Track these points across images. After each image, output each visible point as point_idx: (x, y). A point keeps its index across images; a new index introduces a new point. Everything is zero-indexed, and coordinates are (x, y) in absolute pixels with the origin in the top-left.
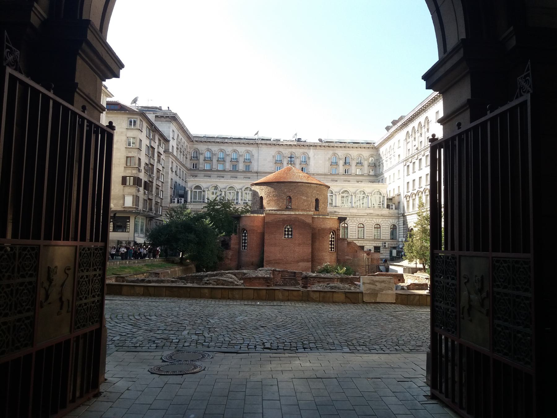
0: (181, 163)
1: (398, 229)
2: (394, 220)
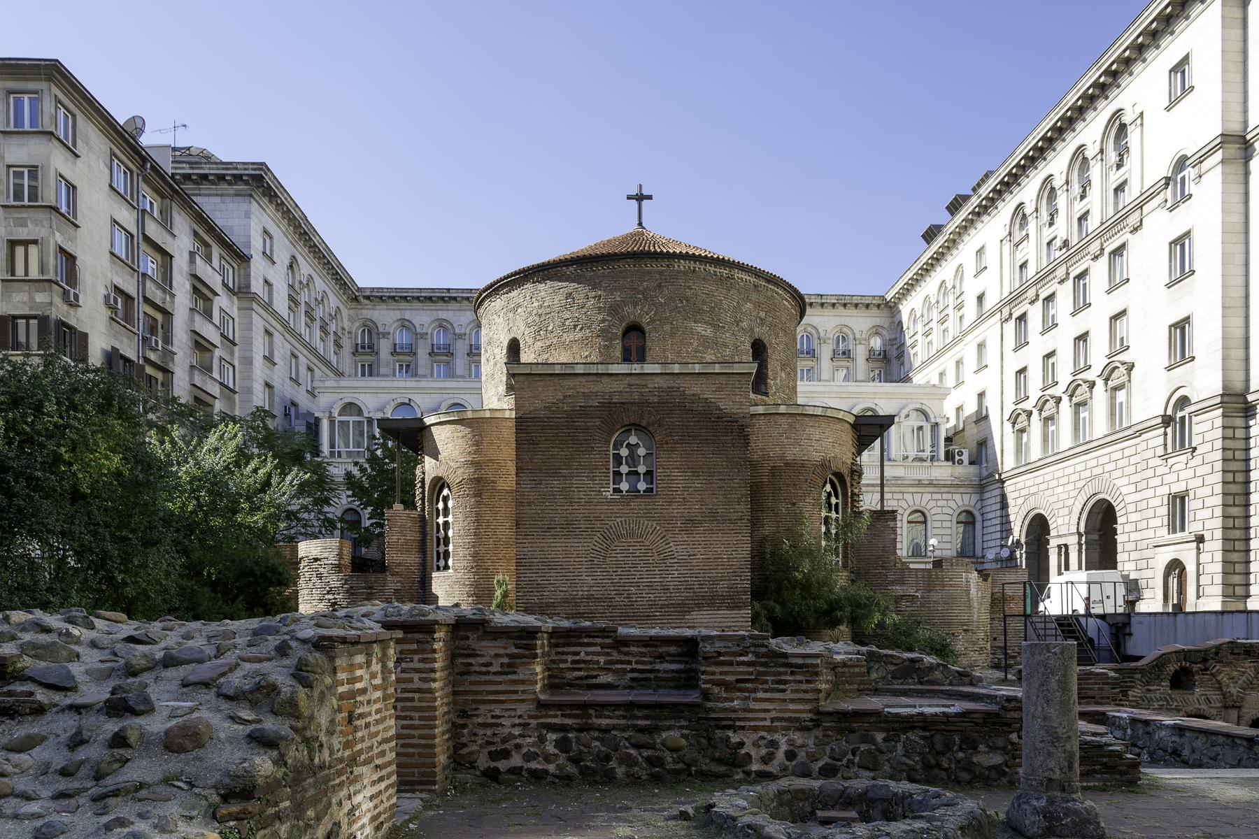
0: (313, 351)
1: (978, 526)
2: (966, 497)
